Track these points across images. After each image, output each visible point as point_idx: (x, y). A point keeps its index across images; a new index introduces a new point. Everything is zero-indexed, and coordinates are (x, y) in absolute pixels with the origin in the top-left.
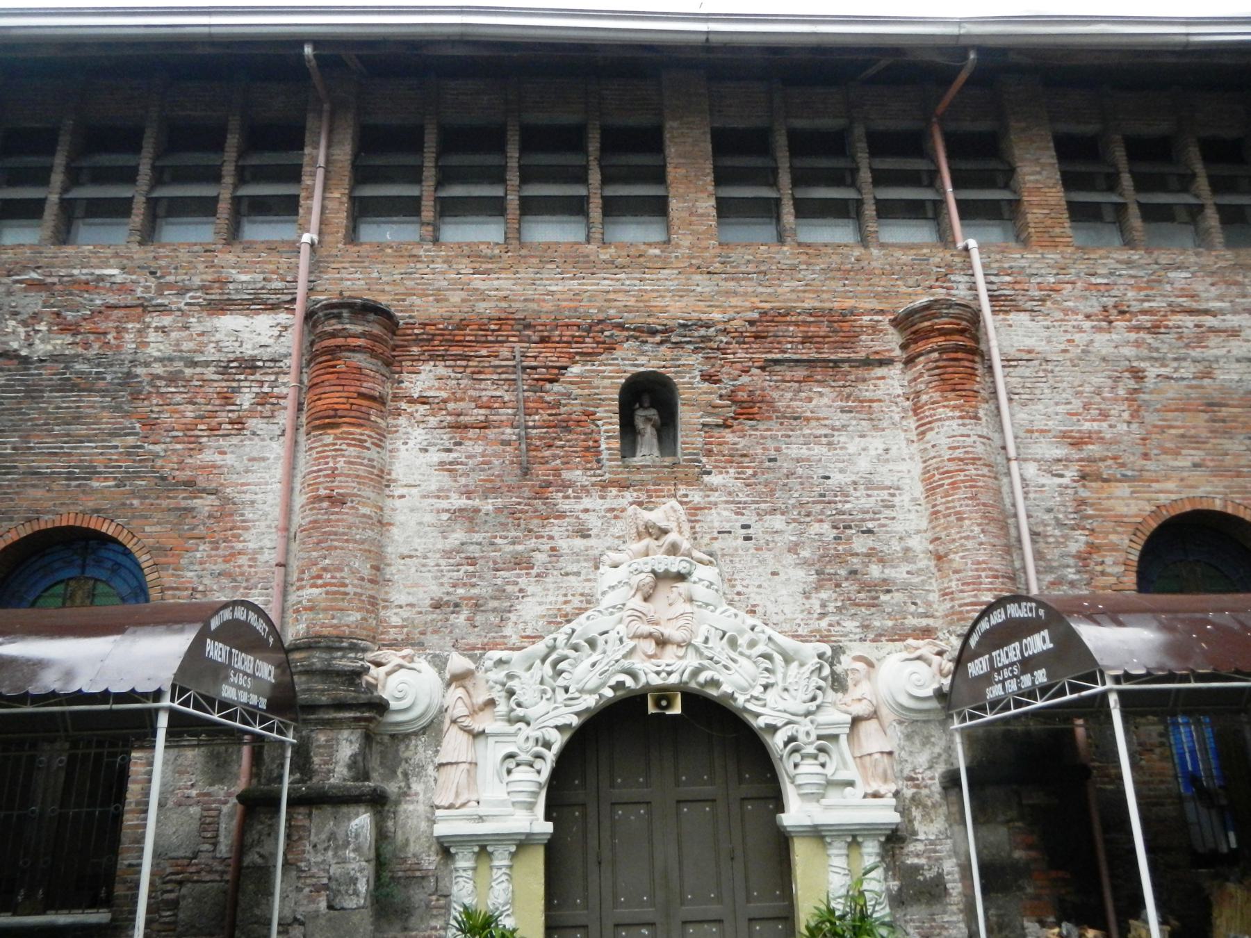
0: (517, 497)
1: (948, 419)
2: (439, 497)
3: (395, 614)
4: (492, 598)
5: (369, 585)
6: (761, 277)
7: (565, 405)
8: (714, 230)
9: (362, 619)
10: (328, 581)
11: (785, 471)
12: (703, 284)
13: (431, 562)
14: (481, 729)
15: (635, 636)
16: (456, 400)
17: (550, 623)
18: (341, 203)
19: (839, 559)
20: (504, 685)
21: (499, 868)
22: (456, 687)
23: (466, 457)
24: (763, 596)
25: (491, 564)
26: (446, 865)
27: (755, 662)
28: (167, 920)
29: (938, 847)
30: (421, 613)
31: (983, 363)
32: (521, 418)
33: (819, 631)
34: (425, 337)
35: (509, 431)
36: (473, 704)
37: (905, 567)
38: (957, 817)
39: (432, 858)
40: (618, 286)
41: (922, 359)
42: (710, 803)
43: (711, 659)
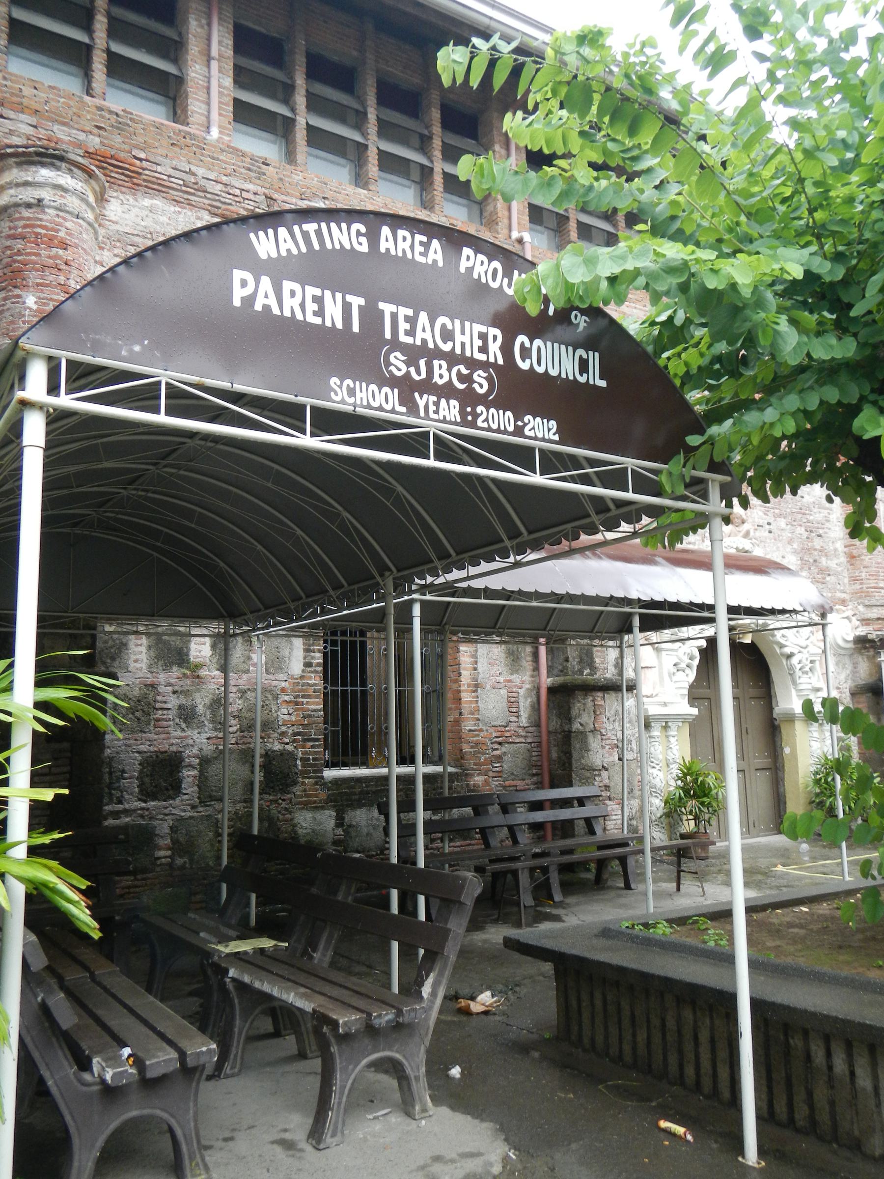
28: (498, 769)
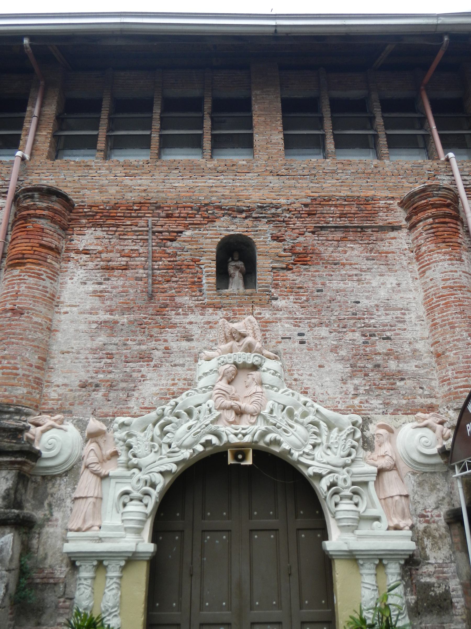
0: (144, 314)
1: (441, 260)
2: (91, 313)
3: (54, 391)
4: (122, 381)
5: (36, 370)
6: (312, 177)
7: (180, 255)
8: (282, 153)
9: (27, 393)
10: (5, 365)
11: (328, 298)
12: (274, 182)
13: (82, 356)
14: (106, 473)
15: (221, 408)
16: (107, 252)
17: (161, 398)
18: (47, 138)
19: (367, 356)
20: (124, 441)
21: (111, 578)
22: (91, 443)
23: (112, 288)
24: (313, 381)
25: (123, 358)
26: (73, 574)
27: (306, 428)
29: (445, 569)
30: (71, 390)
31: (463, 226)
32: (150, 263)
33: (353, 406)
34: (91, 213)
35: (141, 271)
36: (102, 455)
37: (414, 363)
38: (460, 545)
39: (63, 569)
40: (218, 183)
41: (421, 223)
42: (274, 532)
43: (275, 425)
